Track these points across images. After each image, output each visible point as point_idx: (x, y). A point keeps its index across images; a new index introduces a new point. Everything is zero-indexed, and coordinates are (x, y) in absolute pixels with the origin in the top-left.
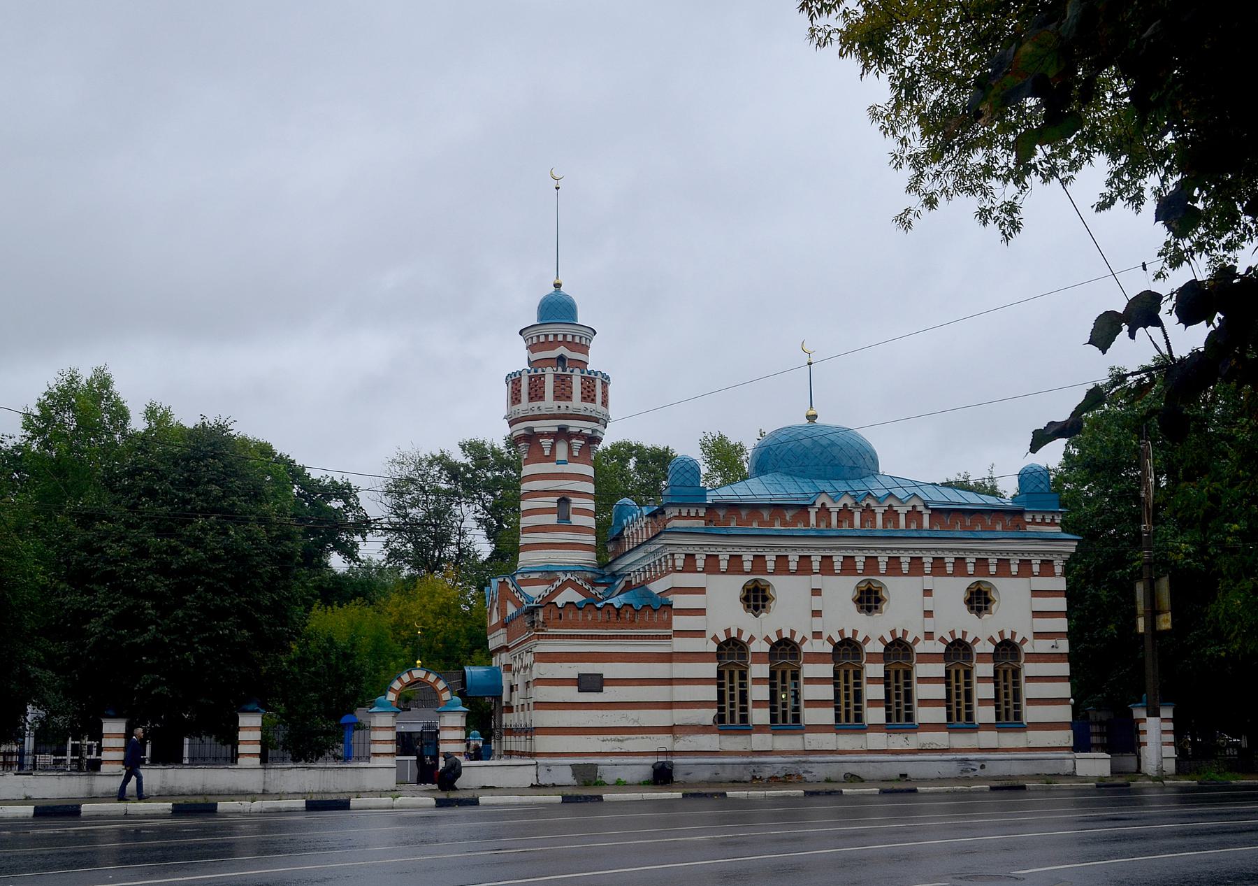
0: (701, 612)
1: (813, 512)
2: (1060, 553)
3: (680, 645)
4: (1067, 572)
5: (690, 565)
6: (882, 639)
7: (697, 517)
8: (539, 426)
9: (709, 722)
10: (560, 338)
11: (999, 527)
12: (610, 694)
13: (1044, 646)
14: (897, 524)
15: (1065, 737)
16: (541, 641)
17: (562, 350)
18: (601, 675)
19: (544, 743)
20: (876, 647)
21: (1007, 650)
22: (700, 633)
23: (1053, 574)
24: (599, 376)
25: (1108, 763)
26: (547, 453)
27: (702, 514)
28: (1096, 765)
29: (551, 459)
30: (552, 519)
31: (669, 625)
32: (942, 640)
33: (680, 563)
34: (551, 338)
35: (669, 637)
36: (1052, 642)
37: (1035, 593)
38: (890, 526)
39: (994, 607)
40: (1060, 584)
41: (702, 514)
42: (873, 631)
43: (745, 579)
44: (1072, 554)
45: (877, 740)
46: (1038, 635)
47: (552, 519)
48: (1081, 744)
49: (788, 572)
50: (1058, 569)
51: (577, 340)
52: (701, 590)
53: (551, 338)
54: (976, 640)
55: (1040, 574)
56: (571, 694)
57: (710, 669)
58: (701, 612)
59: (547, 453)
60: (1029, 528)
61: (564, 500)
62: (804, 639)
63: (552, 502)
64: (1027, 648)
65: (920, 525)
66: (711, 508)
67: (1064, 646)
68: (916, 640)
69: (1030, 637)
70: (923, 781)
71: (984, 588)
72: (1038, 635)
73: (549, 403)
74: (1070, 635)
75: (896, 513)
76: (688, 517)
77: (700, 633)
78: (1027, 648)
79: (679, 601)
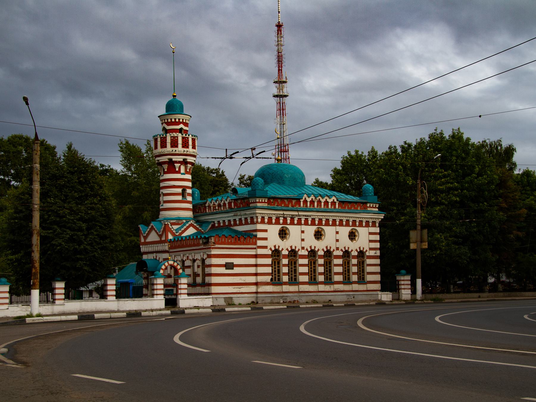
0: (266, 239)
1: (302, 201)
2: (378, 219)
3: (260, 251)
4: (380, 226)
5: (263, 222)
6: (323, 250)
7: (265, 202)
8: (175, 158)
9: (269, 281)
10: (181, 121)
11: (359, 208)
12: (236, 270)
13: (372, 253)
14: (328, 207)
15: (378, 286)
16: (214, 250)
17: (181, 126)
19: (214, 289)
20: (321, 253)
21: (361, 254)
22: (266, 247)
23: (375, 226)
24: (191, 136)
25: (391, 296)
26: (177, 170)
27: (266, 201)
28: (386, 297)
29: (179, 172)
30: (180, 198)
31: (256, 244)
32: (342, 250)
33: (259, 220)
34: (177, 120)
35: (255, 248)
36: (374, 251)
37: (370, 233)
38: (312, 207)
39: (357, 238)
40: (377, 230)
41: (266, 201)
42: (320, 246)
43: (280, 226)
44: (382, 219)
45: (322, 287)
46: (371, 249)
48: (383, 290)
49: (329, 225)
50: (377, 225)
51: (184, 121)
52: (266, 231)
53: (177, 120)
54: (352, 250)
55: (372, 226)
56: (223, 270)
57: (269, 261)
58: (266, 239)
59: (177, 170)
60: (369, 209)
62: (299, 250)
63: (180, 190)
64: (367, 254)
65: (335, 207)
66: (269, 199)
67: (378, 253)
68: (334, 250)
69: (368, 250)
70: (336, 303)
71: (354, 231)
72: (371, 249)
73: (180, 149)
74: (380, 249)
75: (328, 202)
76: (262, 202)
77: (266, 247)
78: (367, 254)
79: (260, 235)
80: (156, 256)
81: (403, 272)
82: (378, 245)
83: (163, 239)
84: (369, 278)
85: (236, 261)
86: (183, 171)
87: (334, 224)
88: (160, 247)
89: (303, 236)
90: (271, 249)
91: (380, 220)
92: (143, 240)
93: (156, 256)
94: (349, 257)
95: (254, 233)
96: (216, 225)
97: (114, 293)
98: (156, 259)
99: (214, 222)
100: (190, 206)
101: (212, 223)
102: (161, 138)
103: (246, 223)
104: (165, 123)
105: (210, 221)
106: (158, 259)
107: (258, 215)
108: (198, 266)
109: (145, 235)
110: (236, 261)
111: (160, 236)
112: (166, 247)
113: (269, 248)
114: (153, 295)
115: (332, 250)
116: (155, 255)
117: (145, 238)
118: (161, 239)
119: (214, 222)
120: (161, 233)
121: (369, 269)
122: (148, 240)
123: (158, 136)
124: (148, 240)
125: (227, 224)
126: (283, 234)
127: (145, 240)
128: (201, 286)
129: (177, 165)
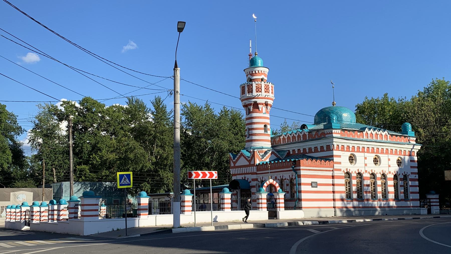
10: (263, 72)
12: (319, 188)
13: (413, 176)
18: (317, 182)
22: (340, 170)
36: (414, 175)
46: (412, 173)
47: (262, 132)
58: (340, 163)
61: (265, 126)
63: (262, 126)
72: (412, 173)
74: (418, 173)
75: (382, 135)
77: (340, 170)
80: (245, 177)
81: (433, 192)
82: (416, 170)
83: (252, 163)
84: (411, 197)
85: (319, 181)
86: (264, 111)
87: (387, 153)
88: (250, 170)
89: (367, 161)
90: (344, 171)
91: (418, 150)
92: (232, 165)
93: (245, 177)
94: (406, 179)
95: (330, 158)
96: (291, 153)
97: (230, 206)
98: (245, 179)
99: (289, 151)
100: (269, 138)
101: (288, 152)
102: (248, 86)
103: (321, 151)
104: (250, 74)
105: (286, 150)
106: (246, 179)
107: (334, 143)
108: (287, 185)
109: (235, 161)
110: (319, 181)
111: (249, 161)
112: (255, 169)
113: (342, 170)
114: (223, 208)
115: (386, 174)
116: (243, 176)
117: (235, 163)
118: (250, 163)
119: (289, 151)
120: (250, 159)
121: (411, 190)
122: (237, 165)
123: (246, 84)
124: (237, 165)
125: (297, 152)
126: (352, 159)
127: (234, 164)
128: (294, 202)
129: (260, 106)
